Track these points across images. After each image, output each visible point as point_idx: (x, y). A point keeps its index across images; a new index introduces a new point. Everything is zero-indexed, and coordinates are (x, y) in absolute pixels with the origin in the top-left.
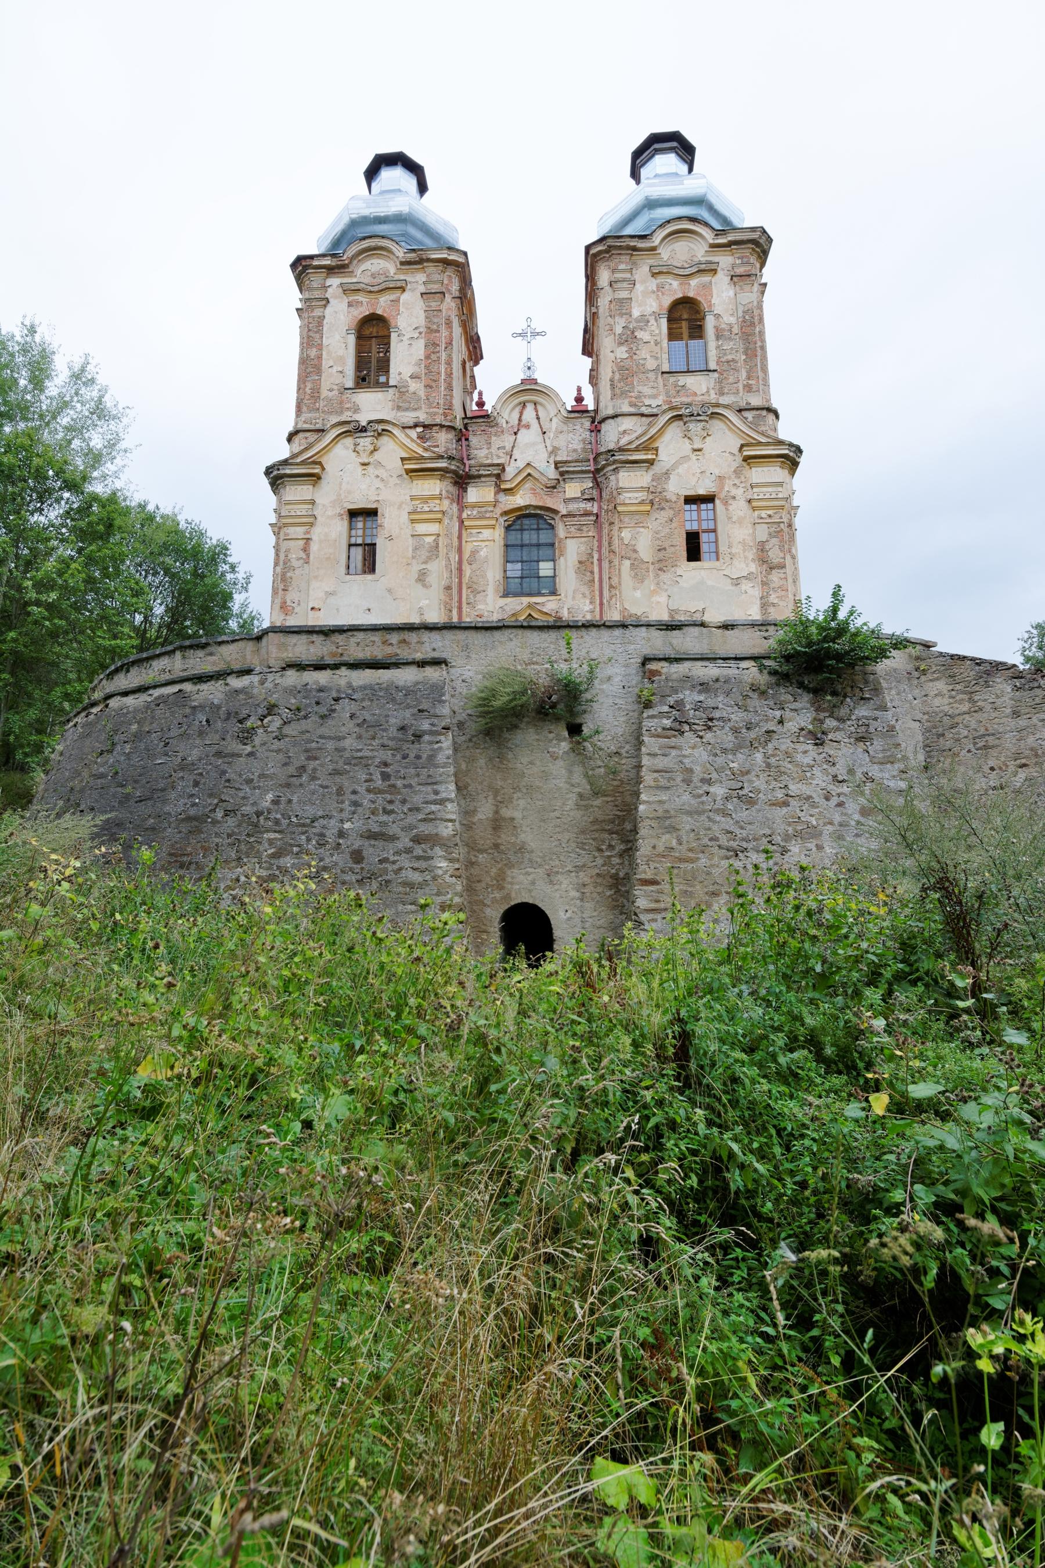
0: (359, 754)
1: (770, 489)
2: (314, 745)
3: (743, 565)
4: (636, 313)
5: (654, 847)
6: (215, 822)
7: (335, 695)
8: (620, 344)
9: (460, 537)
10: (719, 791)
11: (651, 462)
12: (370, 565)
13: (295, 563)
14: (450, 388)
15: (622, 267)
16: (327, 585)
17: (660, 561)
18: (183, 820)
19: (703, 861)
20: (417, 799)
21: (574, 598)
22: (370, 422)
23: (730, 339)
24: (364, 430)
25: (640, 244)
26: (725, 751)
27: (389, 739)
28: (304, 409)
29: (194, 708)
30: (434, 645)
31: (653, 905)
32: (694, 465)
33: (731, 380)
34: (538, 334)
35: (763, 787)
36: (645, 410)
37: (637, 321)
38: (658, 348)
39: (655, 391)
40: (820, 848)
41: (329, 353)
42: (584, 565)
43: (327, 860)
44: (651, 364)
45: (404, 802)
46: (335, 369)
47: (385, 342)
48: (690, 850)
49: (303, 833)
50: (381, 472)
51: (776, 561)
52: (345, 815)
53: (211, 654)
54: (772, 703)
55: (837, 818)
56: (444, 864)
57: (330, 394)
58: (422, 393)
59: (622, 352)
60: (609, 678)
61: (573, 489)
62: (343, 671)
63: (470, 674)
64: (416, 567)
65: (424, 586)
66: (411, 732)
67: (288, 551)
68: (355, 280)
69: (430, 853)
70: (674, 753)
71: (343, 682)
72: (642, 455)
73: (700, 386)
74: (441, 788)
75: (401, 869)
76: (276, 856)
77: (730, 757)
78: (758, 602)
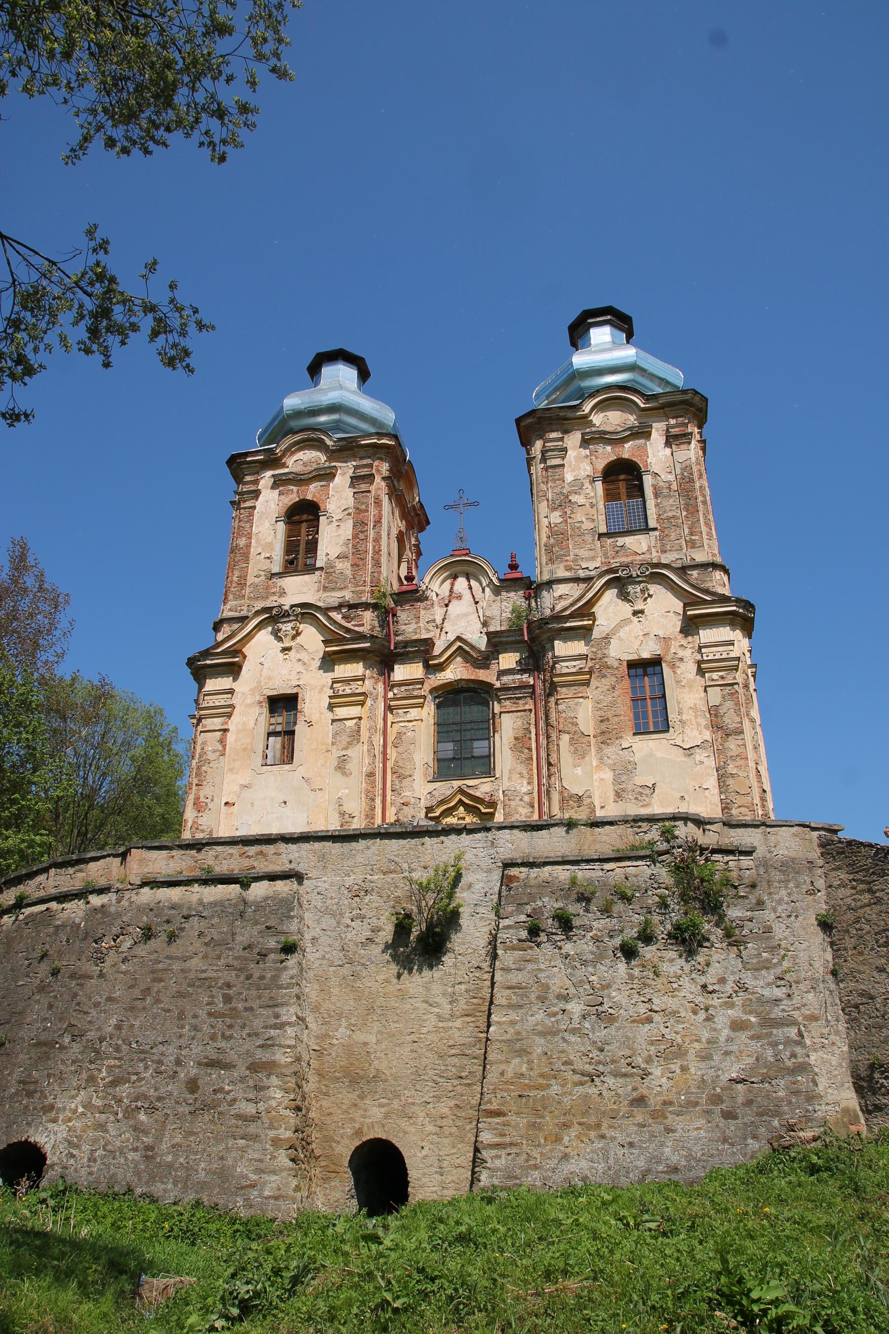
0: (204, 975)
1: (720, 649)
2: (160, 966)
3: (696, 733)
4: (569, 477)
5: (502, 1074)
6: (63, 1048)
7: (185, 913)
8: (554, 509)
9: (385, 719)
10: (576, 1008)
12: (288, 756)
13: (211, 756)
14: (377, 564)
15: (554, 435)
16: (244, 777)
17: (603, 733)
18: (34, 1045)
19: (555, 1089)
20: (258, 1023)
21: (510, 778)
22: (292, 606)
23: (669, 496)
24: (286, 614)
25: (569, 414)
26: (584, 963)
27: (236, 958)
28: (231, 597)
29: (57, 927)
30: (291, 857)
31: (497, 1140)
32: (636, 627)
33: (673, 537)
34: (470, 505)
35: (624, 1002)
36: (582, 574)
38: (594, 510)
39: (592, 553)
40: (684, 1069)
41: (258, 541)
42: (521, 743)
43: (162, 1090)
44: (587, 525)
45: (243, 1026)
46: (263, 555)
47: (314, 524)
48: (542, 1075)
49: (142, 1061)
50: (303, 656)
51: (732, 726)
52: (183, 1042)
53: (80, 871)
54: (637, 907)
55: (705, 1035)
56: (279, 1094)
57: (257, 580)
58: (349, 573)
59: (556, 517)
60: (470, 886)
61: (508, 660)
62: (196, 887)
63: (326, 886)
64: (336, 753)
65: (344, 774)
66: (256, 951)
67: (204, 743)
68: (286, 470)
69: (266, 1082)
70: (530, 966)
71: (194, 898)
72: (579, 622)
73: (639, 545)
74: (282, 1011)
75: (234, 1100)
76: (114, 1083)
77: (590, 969)
78: (715, 774)
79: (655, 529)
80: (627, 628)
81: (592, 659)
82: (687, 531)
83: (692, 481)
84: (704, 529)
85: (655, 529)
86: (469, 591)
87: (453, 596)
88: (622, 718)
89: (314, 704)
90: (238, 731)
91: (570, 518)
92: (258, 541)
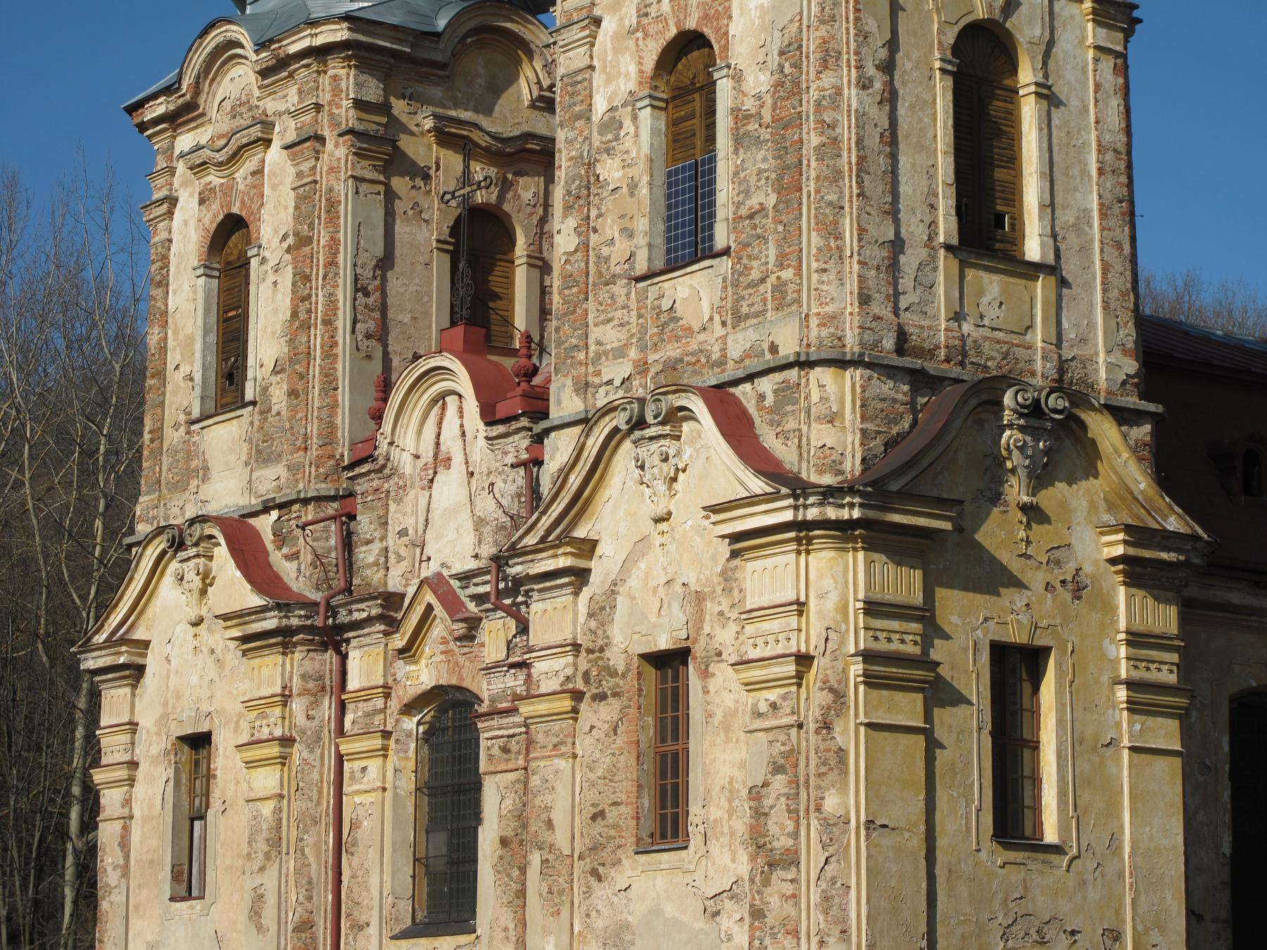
4: (600, 105)
11: (580, 576)
14: (330, 385)
23: (758, 142)
37: (605, 127)
39: (622, 335)
64: (250, 883)
65: (260, 928)
79: (726, 252)
80: (642, 565)
81: (590, 651)
82: (772, 252)
83: (796, 83)
84: (812, 241)
85: (726, 252)
86: (460, 442)
87: (441, 460)
88: (623, 809)
89: (225, 759)
90: (145, 820)
91: (595, 231)
92: (175, 333)
